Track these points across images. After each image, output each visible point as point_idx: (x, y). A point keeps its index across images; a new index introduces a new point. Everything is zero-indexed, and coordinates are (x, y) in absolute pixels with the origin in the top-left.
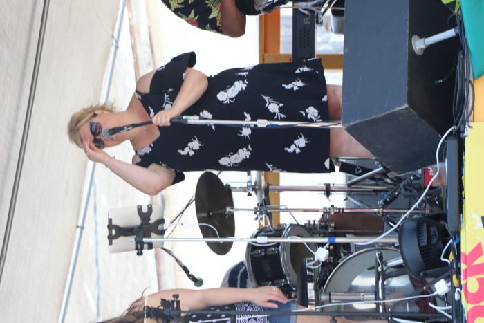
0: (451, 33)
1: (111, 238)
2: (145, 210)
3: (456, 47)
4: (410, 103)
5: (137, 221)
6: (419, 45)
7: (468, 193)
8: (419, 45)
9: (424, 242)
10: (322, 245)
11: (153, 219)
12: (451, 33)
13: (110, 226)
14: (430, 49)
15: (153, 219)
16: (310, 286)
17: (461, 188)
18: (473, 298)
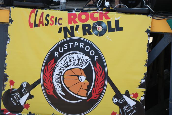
17: (131, 13)
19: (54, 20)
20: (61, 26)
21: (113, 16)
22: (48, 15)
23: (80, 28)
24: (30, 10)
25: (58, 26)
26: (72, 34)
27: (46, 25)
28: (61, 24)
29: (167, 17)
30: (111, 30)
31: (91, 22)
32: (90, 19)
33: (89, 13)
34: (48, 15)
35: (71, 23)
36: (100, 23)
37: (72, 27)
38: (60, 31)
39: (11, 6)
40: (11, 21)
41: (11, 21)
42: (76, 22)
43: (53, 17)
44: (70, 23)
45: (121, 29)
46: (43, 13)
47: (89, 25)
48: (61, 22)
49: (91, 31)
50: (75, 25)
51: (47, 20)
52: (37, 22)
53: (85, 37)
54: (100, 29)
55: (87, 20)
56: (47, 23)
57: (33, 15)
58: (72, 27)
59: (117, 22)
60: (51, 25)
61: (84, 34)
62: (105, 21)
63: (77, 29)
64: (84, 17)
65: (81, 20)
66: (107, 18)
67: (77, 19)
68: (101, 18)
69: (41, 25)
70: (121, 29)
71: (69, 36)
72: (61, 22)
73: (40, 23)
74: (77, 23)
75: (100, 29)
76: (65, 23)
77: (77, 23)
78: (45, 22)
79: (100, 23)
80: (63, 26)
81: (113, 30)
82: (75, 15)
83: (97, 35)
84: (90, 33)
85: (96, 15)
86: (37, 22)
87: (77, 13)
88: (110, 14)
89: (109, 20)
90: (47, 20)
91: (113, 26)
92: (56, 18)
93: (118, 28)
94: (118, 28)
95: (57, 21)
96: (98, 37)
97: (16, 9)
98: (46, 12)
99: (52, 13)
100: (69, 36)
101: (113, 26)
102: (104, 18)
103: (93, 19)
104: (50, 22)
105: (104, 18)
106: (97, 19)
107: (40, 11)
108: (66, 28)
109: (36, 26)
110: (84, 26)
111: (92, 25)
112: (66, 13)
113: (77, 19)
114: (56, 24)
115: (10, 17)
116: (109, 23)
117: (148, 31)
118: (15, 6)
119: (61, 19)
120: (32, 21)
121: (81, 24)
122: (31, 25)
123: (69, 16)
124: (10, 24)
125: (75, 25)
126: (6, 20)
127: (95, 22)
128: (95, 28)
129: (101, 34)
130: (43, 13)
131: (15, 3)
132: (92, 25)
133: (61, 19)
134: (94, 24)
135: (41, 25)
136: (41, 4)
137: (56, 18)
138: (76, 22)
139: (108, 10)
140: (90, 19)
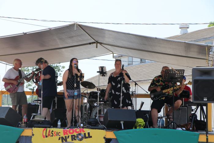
0: (123, 128)
1: (101, 67)
2: (106, 73)
3: (121, 129)
4: (109, 121)
5: (104, 72)
6: (122, 122)
7: (94, 130)
8: (122, 122)
9: (92, 123)
10: (97, 104)
11: (105, 74)
12: (123, 128)
13: (103, 67)
14: (121, 124)
15: (105, 74)
16: (103, 103)
17: (95, 129)
18: (76, 130)
19: (56, 133)
20: (60, 137)
21: (87, 131)
22: (53, 131)
23: (70, 137)
24: (43, 129)
25: (58, 137)
26: (66, 140)
27: (52, 136)
28: (60, 136)
29: (113, 130)
30: (86, 138)
31: (75, 134)
32: (75, 133)
33: (74, 129)
34: (53, 131)
35: (65, 135)
36: (80, 134)
37: (66, 137)
38: (59, 139)
39: (32, 127)
40: (33, 135)
41: (33, 135)
42: (67, 134)
43: (55, 132)
44: (64, 135)
45: (91, 137)
46: (50, 130)
47: (74, 136)
48: (59, 134)
49: (76, 138)
50: (67, 136)
51: (52, 133)
52: (47, 135)
53: (72, 141)
54: (80, 137)
55: (73, 132)
56: (52, 135)
57: (45, 131)
58: (66, 137)
59: (89, 133)
60: (55, 136)
61: (72, 140)
62: (83, 133)
63: (68, 138)
64: (71, 131)
65: (70, 133)
66: (84, 131)
67: (68, 133)
68: (81, 132)
69: (49, 136)
70: (91, 137)
71: (64, 141)
72: (59, 134)
73: (49, 135)
74: (68, 134)
75: (80, 137)
76: (62, 135)
77: (68, 134)
78: (51, 135)
79: (80, 134)
80: (61, 136)
81: (87, 138)
82: (67, 130)
83: (79, 140)
84: (75, 140)
85: (78, 130)
86: (47, 135)
87: (68, 130)
88: (85, 129)
89: (85, 133)
90: (52, 133)
91: (87, 135)
92: (57, 132)
93: (90, 137)
94: (90, 137)
95: (58, 134)
96: (79, 141)
97: (35, 128)
98: (52, 129)
99: (55, 130)
100: (64, 141)
101: (87, 135)
102: (82, 131)
103: (76, 132)
104: (54, 135)
105: (82, 131)
106: (78, 132)
107: (48, 129)
108: (62, 138)
109: (46, 137)
110: (72, 136)
111: (76, 135)
112: (62, 129)
113: (68, 133)
114: (57, 136)
115: (32, 133)
116: (85, 134)
117: (104, 138)
118: (34, 127)
119: (60, 133)
120: (44, 134)
121: (70, 135)
122: (44, 137)
123: (64, 132)
124: (33, 136)
125: (67, 136)
126: (31, 135)
127: (77, 134)
128: (77, 137)
129: (81, 140)
130: (50, 130)
131: (35, 125)
132: (76, 135)
133: (60, 133)
134: (77, 135)
135: (49, 136)
136: (49, 126)
137: (57, 132)
138: (67, 134)
139: (83, 128)
140: (75, 133)
